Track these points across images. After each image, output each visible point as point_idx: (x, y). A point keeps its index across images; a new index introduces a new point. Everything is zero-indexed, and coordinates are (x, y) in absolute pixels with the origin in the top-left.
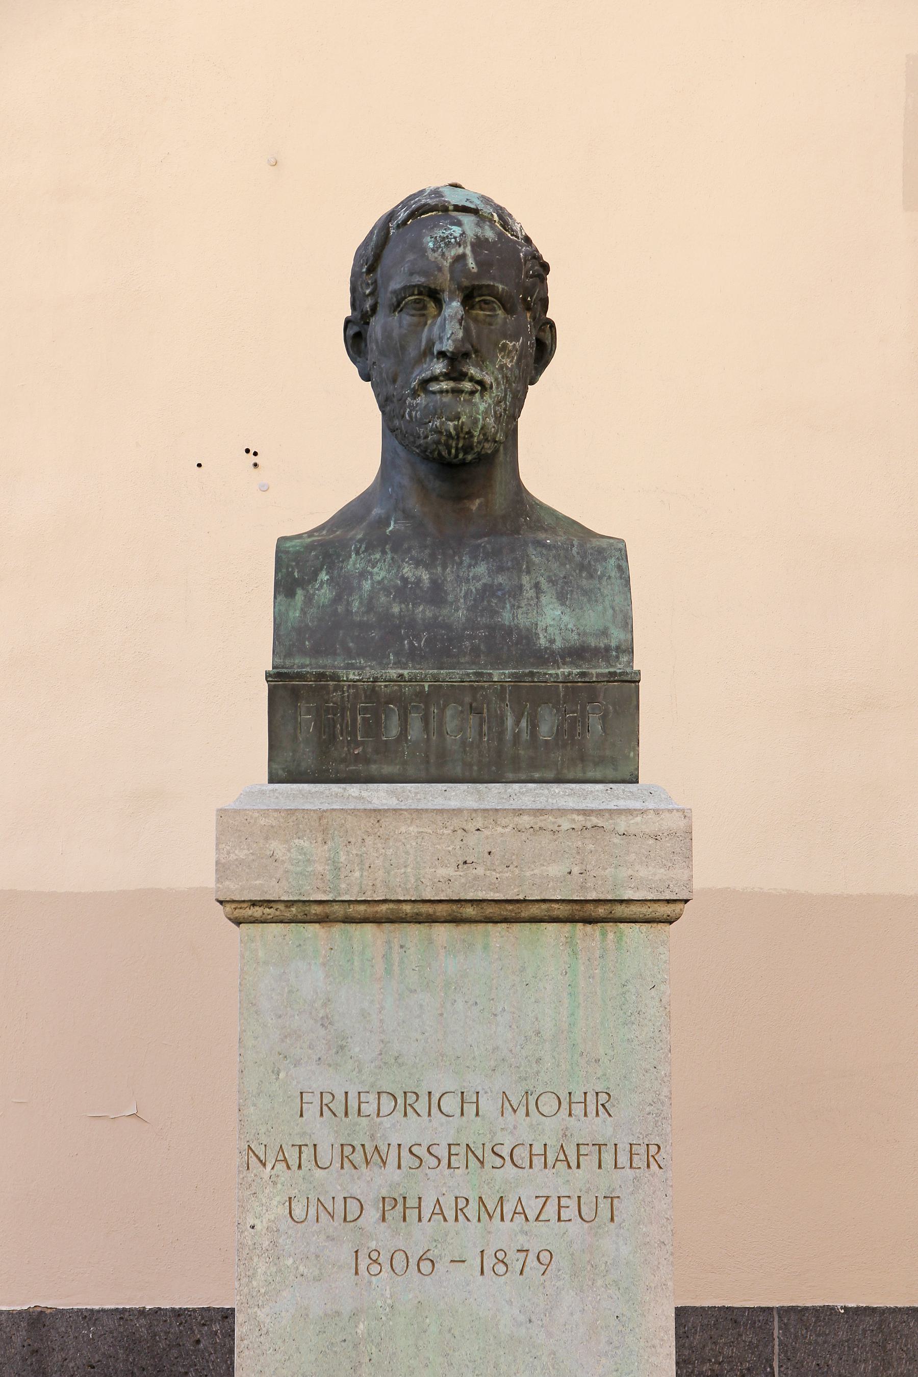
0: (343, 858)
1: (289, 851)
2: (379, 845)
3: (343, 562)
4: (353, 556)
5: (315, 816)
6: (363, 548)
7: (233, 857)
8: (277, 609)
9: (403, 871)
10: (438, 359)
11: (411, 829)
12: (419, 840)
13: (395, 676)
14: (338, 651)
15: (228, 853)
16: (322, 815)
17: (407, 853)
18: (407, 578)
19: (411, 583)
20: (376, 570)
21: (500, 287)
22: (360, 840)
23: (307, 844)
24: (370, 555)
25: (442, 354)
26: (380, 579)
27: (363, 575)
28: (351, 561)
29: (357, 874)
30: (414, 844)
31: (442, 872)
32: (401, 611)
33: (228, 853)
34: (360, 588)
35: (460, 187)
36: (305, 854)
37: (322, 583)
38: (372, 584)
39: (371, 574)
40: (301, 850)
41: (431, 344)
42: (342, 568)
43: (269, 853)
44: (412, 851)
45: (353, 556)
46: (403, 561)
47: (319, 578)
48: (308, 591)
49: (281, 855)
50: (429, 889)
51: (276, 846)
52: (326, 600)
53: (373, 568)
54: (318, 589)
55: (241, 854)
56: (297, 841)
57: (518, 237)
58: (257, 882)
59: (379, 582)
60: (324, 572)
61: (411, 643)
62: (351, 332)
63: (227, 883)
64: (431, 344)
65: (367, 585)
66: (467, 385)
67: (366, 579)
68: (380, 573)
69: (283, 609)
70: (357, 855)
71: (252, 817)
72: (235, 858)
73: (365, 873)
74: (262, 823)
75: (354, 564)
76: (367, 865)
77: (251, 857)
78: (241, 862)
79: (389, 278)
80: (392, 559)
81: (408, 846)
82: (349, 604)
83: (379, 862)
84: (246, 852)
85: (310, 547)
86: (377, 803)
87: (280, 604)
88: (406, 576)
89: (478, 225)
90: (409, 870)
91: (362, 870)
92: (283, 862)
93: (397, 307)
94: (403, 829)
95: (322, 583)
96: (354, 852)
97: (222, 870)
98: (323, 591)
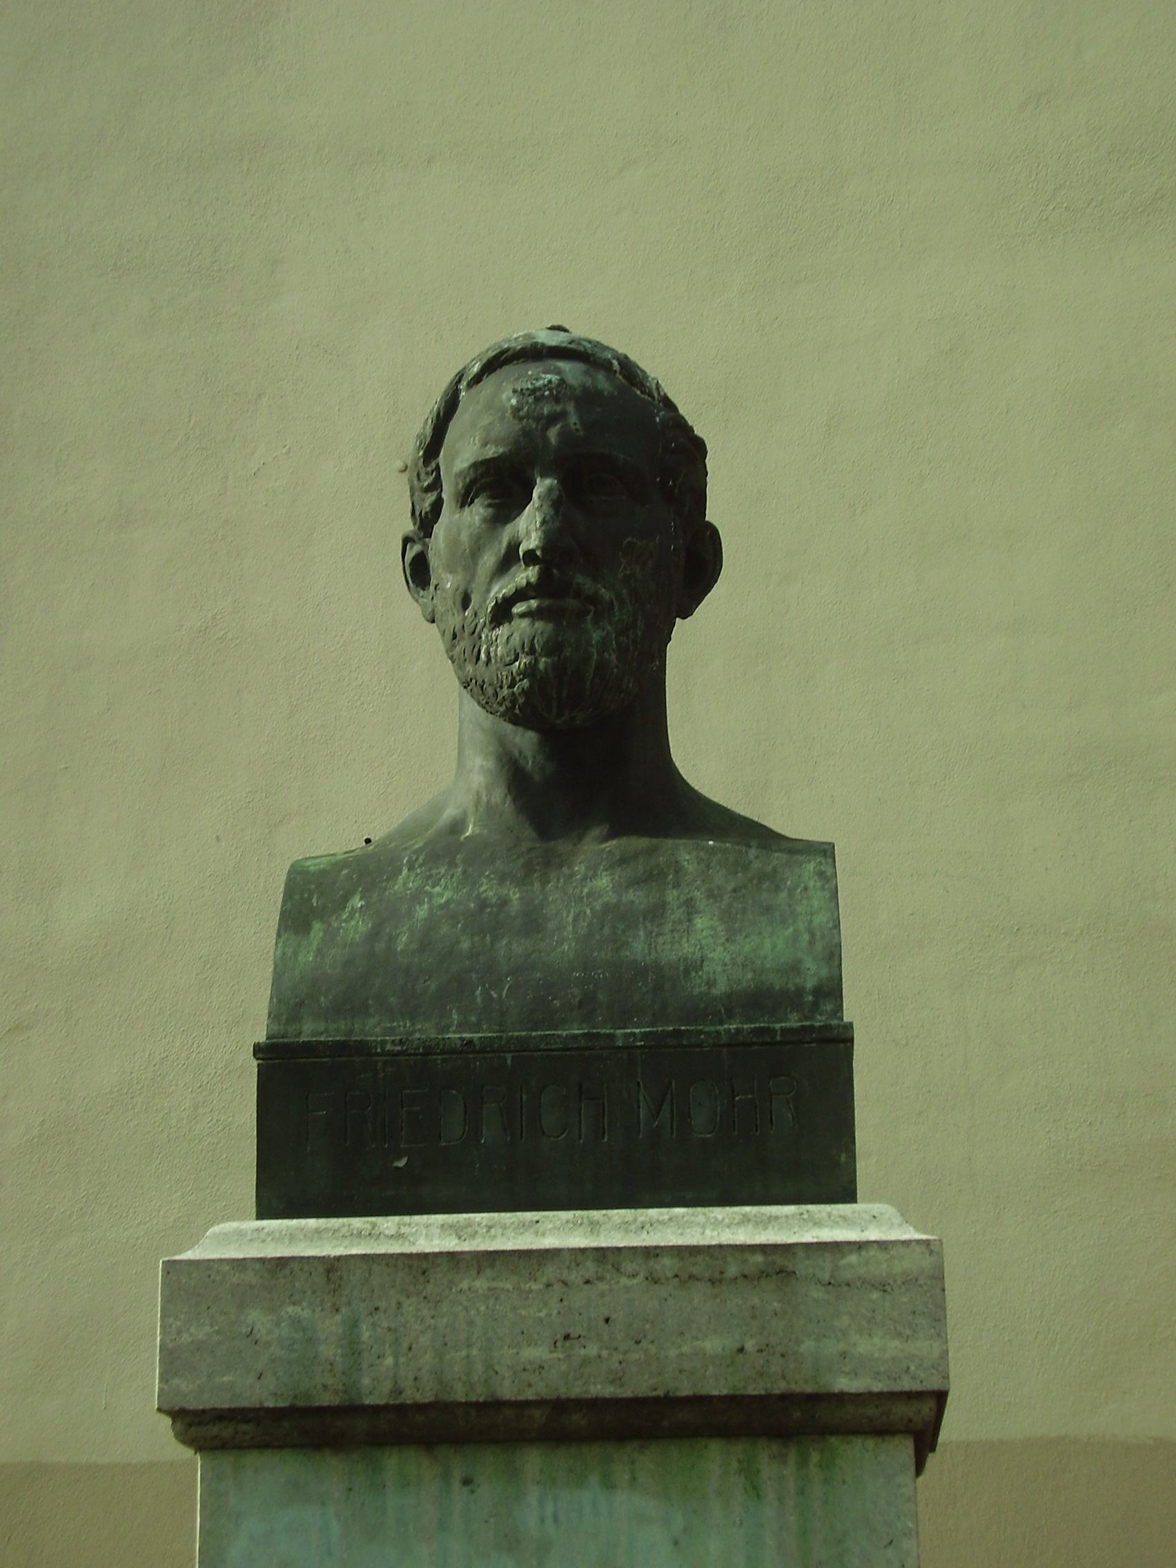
0: (365, 1334)
1: (278, 1325)
2: (425, 1312)
3: (388, 880)
4: (405, 871)
5: (321, 1269)
6: (421, 860)
7: (186, 1338)
8: (279, 953)
9: (464, 1353)
10: (527, 565)
11: (478, 1284)
12: (491, 1302)
13: (459, 1043)
14: (372, 1010)
15: (179, 1332)
16: (331, 1266)
17: (471, 1323)
18: (486, 899)
19: (492, 906)
20: (438, 889)
21: (621, 456)
22: (394, 1305)
23: (306, 1314)
24: (430, 869)
25: (530, 558)
26: (443, 901)
27: (417, 897)
28: (401, 879)
29: (389, 1361)
30: (483, 1308)
31: (532, 1353)
32: (473, 946)
33: (179, 1332)
34: (410, 913)
35: (565, 330)
36: (304, 1330)
37: (353, 911)
38: (430, 909)
39: (431, 896)
40: (296, 1322)
41: (513, 547)
42: (385, 889)
43: (244, 1330)
44: (479, 1321)
45: (405, 871)
46: (481, 875)
47: (349, 905)
48: (330, 925)
49: (264, 1332)
50: (507, 1383)
51: (256, 1317)
52: (357, 936)
53: (433, 887)
54: (345, 921)
55: (200, 1333)
56: (290, 1309)
57: (653, 398)
58: (226, 1379)
59: (441, 907)
60: (357, 897)
61: (486, 993)
62: (409, 556)
63: (176, 1381)
64: (513, 547)
65: (422, 912)
66: (571, 603)
67: (421, 903)
68: (443, 893)
69: (289, 952)
70: (389, 1329)
71: (218, 1272)
72: (190, 1340)
73: (402, 1360)
74: (235, 1280)
75: (405, 882)
76: (406, 1345)
77: (216, 1338)
78: (199, 1347)
79: (453, 456)
80: (464, 872)
81: (473, 1312)
82: (392, 939)
83: (425, 1340)
84: (207, 1329)
85: (344, 864)
86: (424, 1245)
87: (285, 946)
88: (484, 895)
89: (586, 373)
90: (475, 1352)
91: (396, 1356)
92: (268, 1344)
93: (465, 500)
94: (465, 1285)
95: (353, 911)
96: (385, 1324)
97: (172, 1360)
98: (353, 923)
